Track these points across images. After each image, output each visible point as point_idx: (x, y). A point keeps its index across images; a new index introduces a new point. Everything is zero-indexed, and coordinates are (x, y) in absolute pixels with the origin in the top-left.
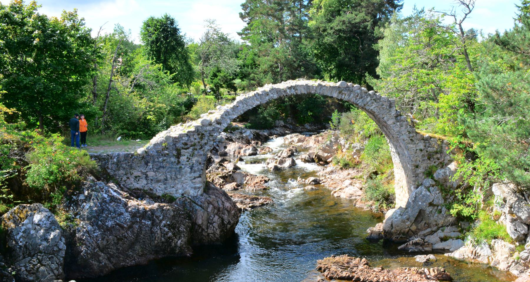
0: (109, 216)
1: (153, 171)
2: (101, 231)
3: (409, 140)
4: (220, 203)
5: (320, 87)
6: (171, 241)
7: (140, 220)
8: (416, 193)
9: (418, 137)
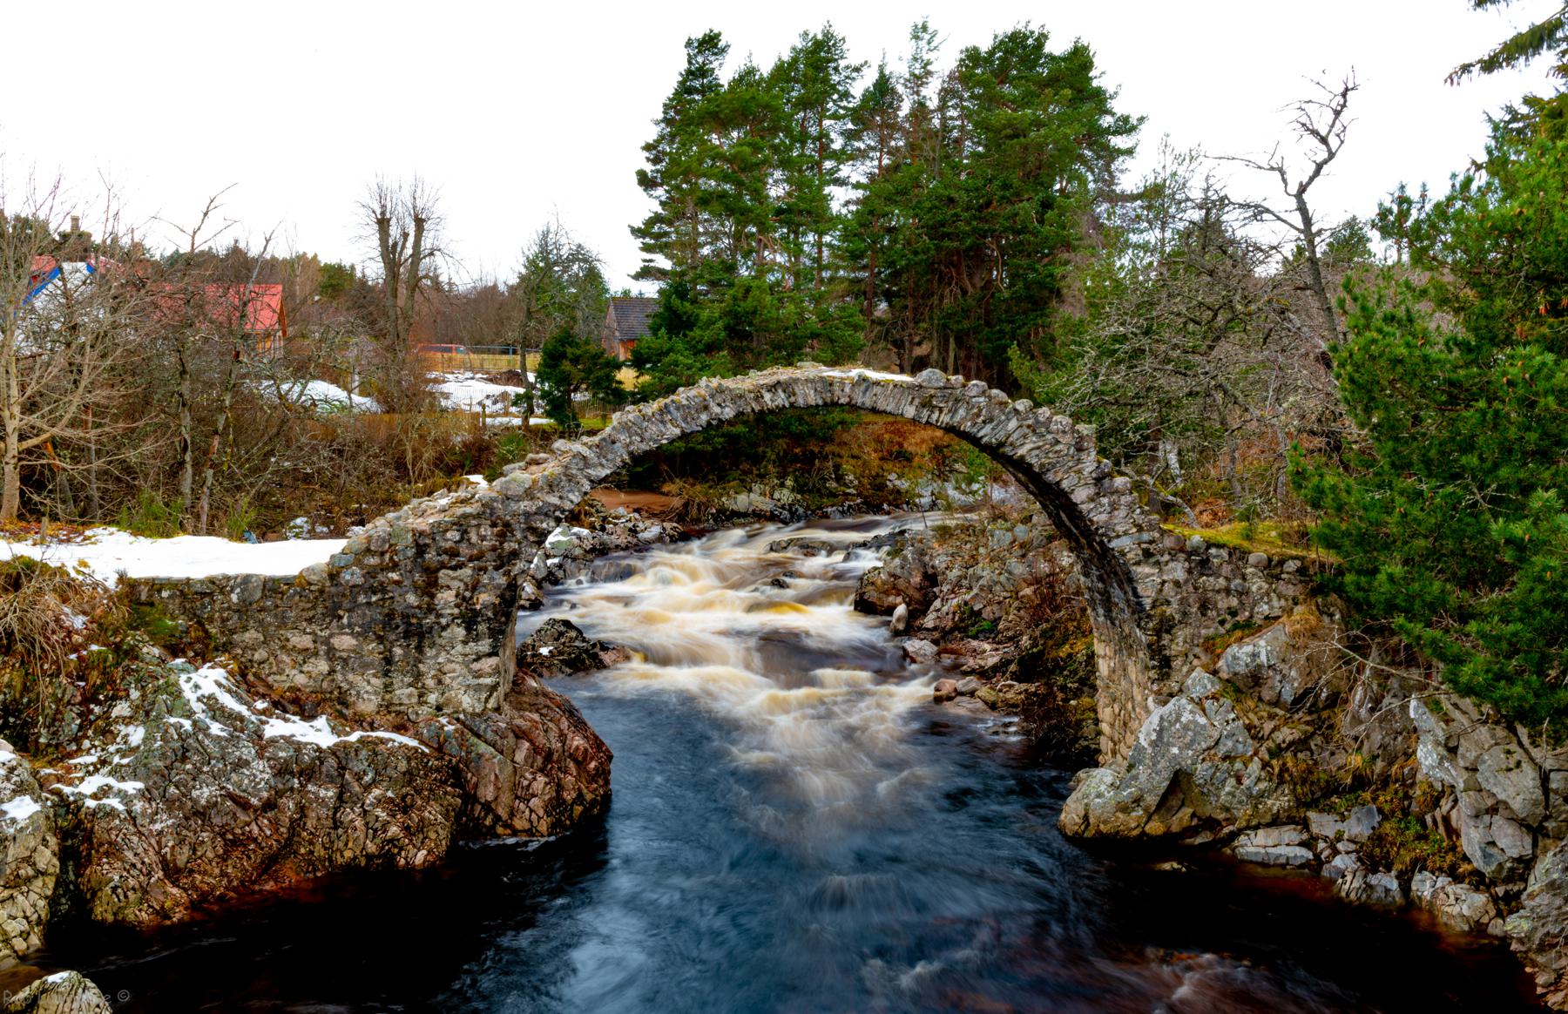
0: (205, 769)
1: (352, 634)
2: (176, 817)
3: (1140, 552)
4: (553, 735)
5: (863, 387)
6: (396, 851)
8: (1162, 718)
9: (1169, 542)
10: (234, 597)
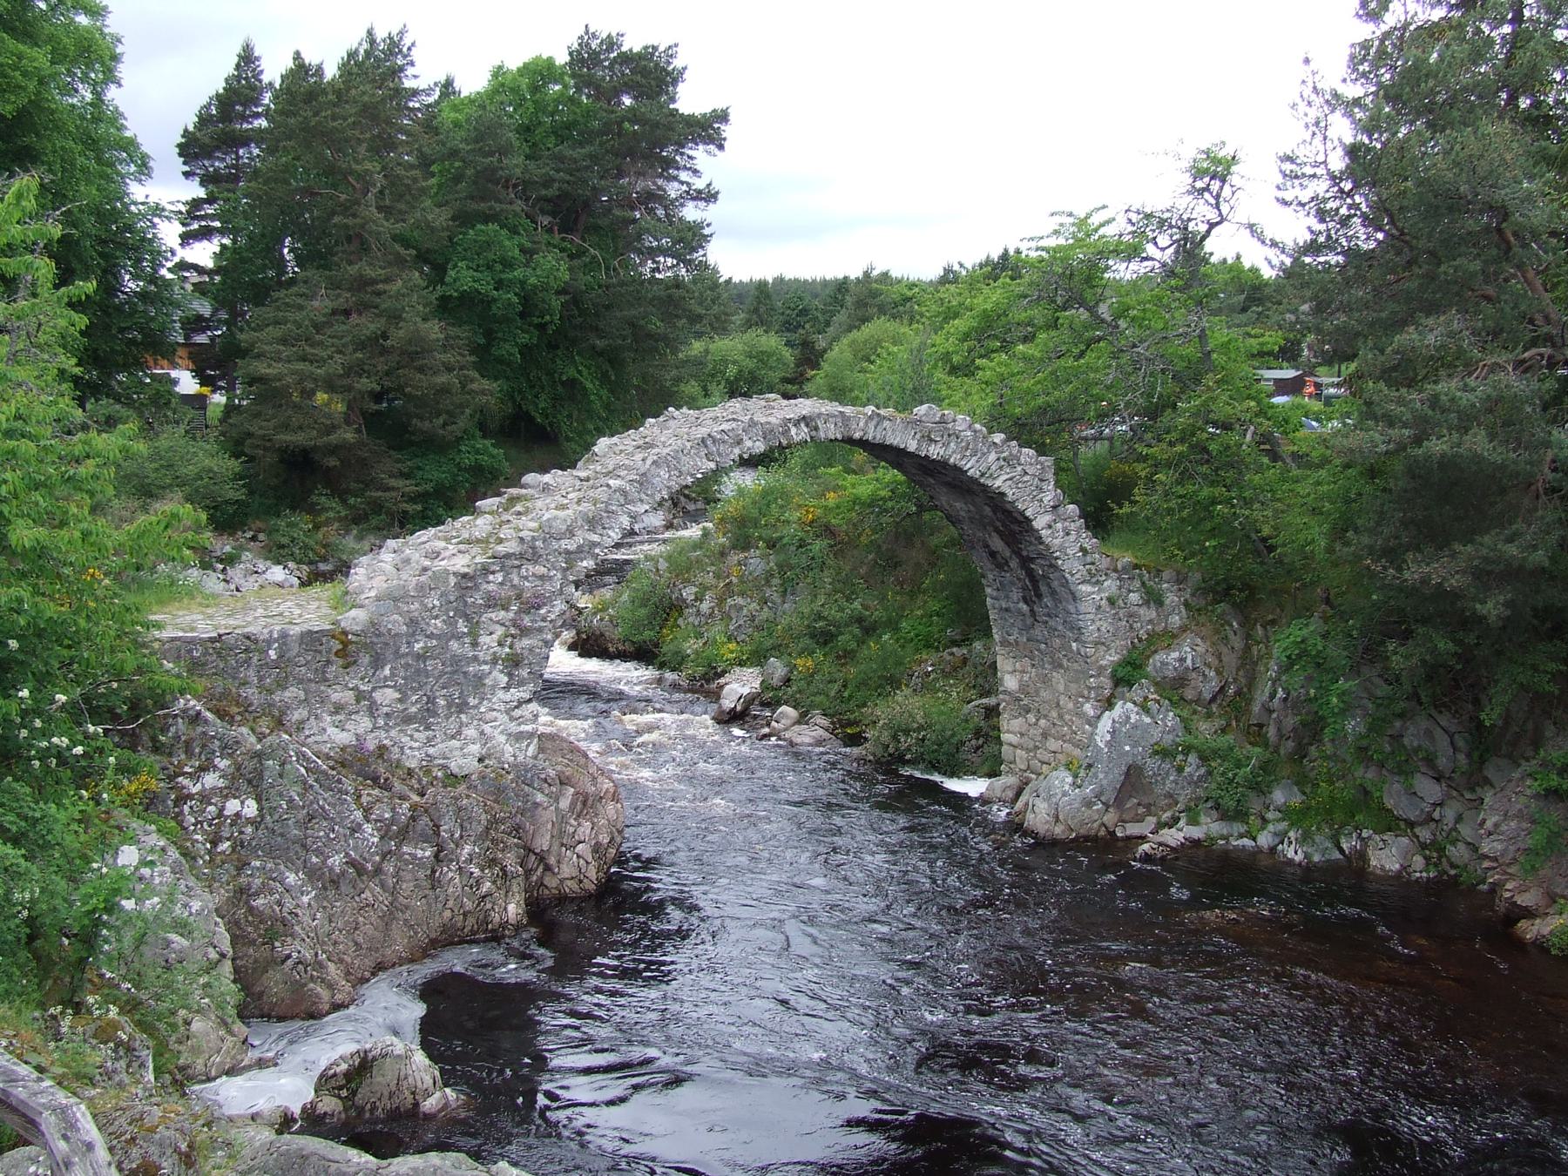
1: (394, 686)
5: (874, 422)
7: (399, 846)
10: (272, 653)
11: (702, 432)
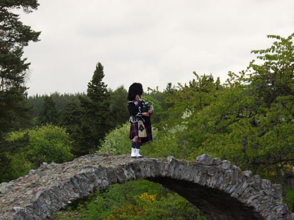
5: (174, 166)
11: (69, 175)
